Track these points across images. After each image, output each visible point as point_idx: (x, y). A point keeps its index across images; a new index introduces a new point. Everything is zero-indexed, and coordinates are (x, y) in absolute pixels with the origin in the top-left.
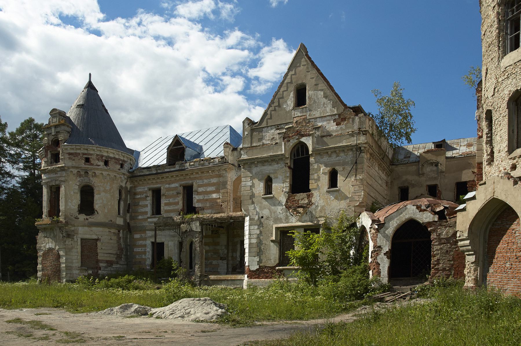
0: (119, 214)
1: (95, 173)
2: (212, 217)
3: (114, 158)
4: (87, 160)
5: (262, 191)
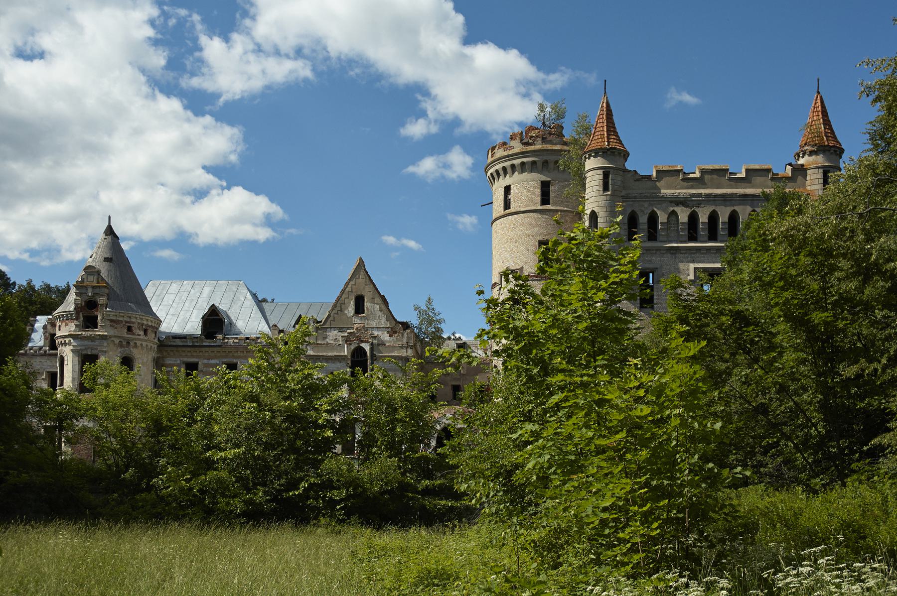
4: (129, 329)
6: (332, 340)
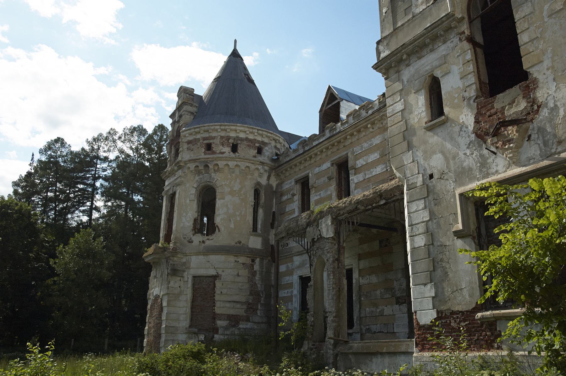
0: (255, 229)
1: (217, 165)
2: (351, 201)
3: (247, 139)
4: (209, 147)
5: (424, 114)
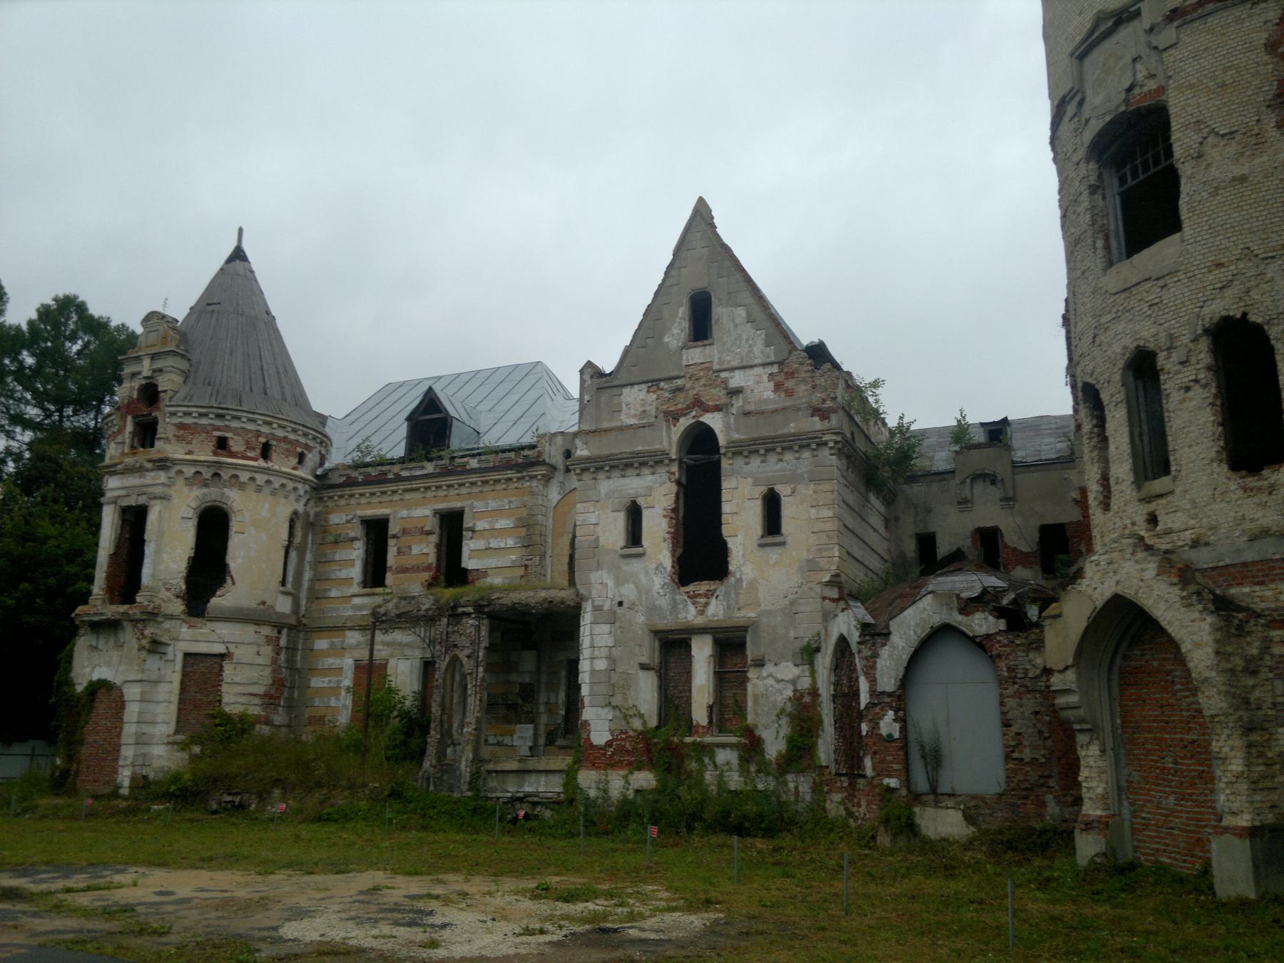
6: (635, 416)
